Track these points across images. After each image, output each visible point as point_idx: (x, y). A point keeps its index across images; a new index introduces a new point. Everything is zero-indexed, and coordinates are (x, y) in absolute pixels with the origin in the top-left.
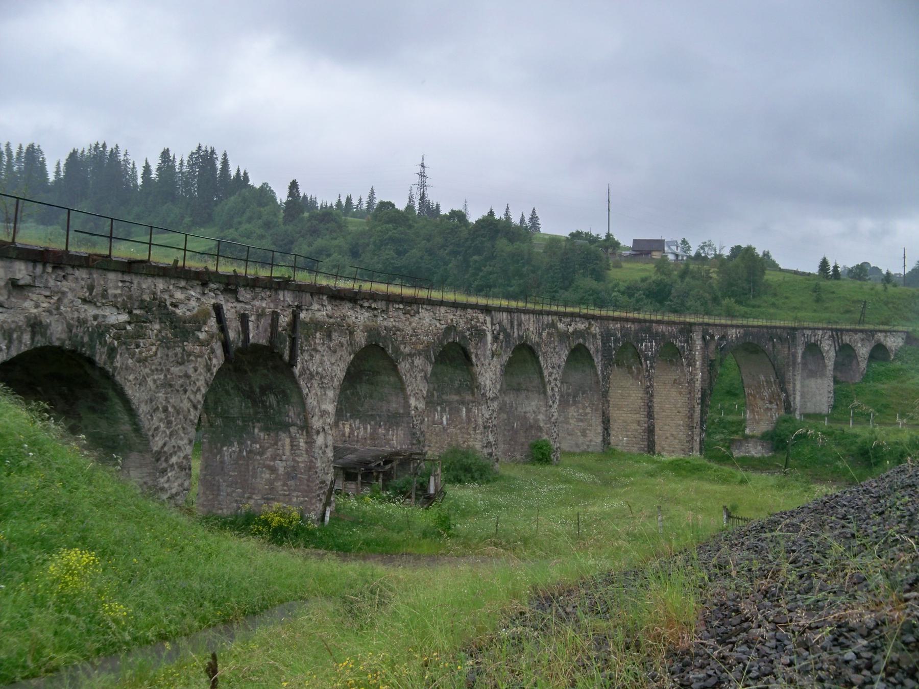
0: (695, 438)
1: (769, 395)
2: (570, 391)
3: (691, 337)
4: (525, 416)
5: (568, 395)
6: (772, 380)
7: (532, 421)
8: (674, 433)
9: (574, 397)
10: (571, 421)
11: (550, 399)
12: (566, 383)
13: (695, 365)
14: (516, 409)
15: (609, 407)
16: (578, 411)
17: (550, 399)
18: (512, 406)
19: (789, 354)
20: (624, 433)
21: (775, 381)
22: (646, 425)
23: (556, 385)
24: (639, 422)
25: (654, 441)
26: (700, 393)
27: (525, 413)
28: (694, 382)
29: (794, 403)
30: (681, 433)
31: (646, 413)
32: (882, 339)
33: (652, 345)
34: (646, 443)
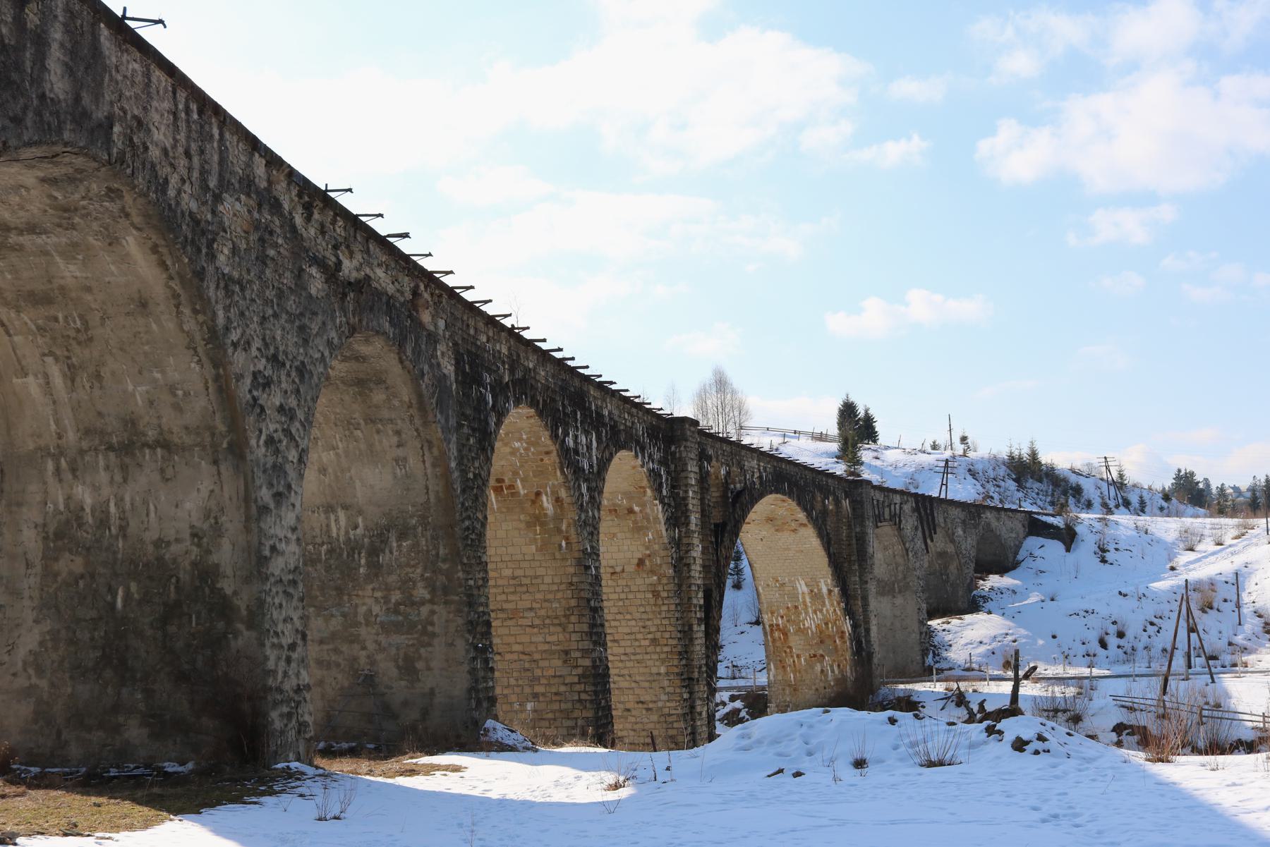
0: (698, 709)
1: (818, 626)
2: (359, 531)
3: (673, 454)
4: (160, 559)
5: (354, 547)
6: (825, 590)
7: (184, 577)
8: (647, 698)
9: (374, 552)
10: (363, 631)
11: (260, 479)
12: (345, 507)
13: (688, 524)
14: (123, 529)
15: (485, 580)
16: (386, 600)
17: (260, 479)
18: (103, 522)
19: (849, 536)
20: (527, 690)
21: (830, 591)
22: (587, 662)
23: (287, 432)
24: (567, 652)
25: (609, 708)
26: (701, 595)
27: (159, 543)
28: (688, 565)
29: (868, 642)
30: (664, 697)
31: (585, 628)
32: (994, 524)
33: (589, 447)
34: (590, 714)
